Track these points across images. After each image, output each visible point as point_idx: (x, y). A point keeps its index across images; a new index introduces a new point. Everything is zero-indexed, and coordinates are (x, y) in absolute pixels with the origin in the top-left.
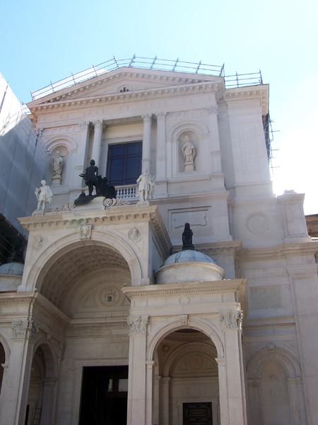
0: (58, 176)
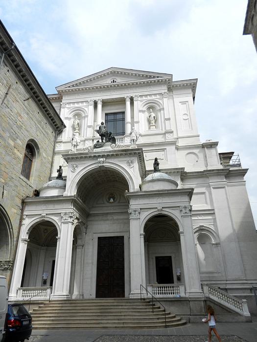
0: (78, 131)
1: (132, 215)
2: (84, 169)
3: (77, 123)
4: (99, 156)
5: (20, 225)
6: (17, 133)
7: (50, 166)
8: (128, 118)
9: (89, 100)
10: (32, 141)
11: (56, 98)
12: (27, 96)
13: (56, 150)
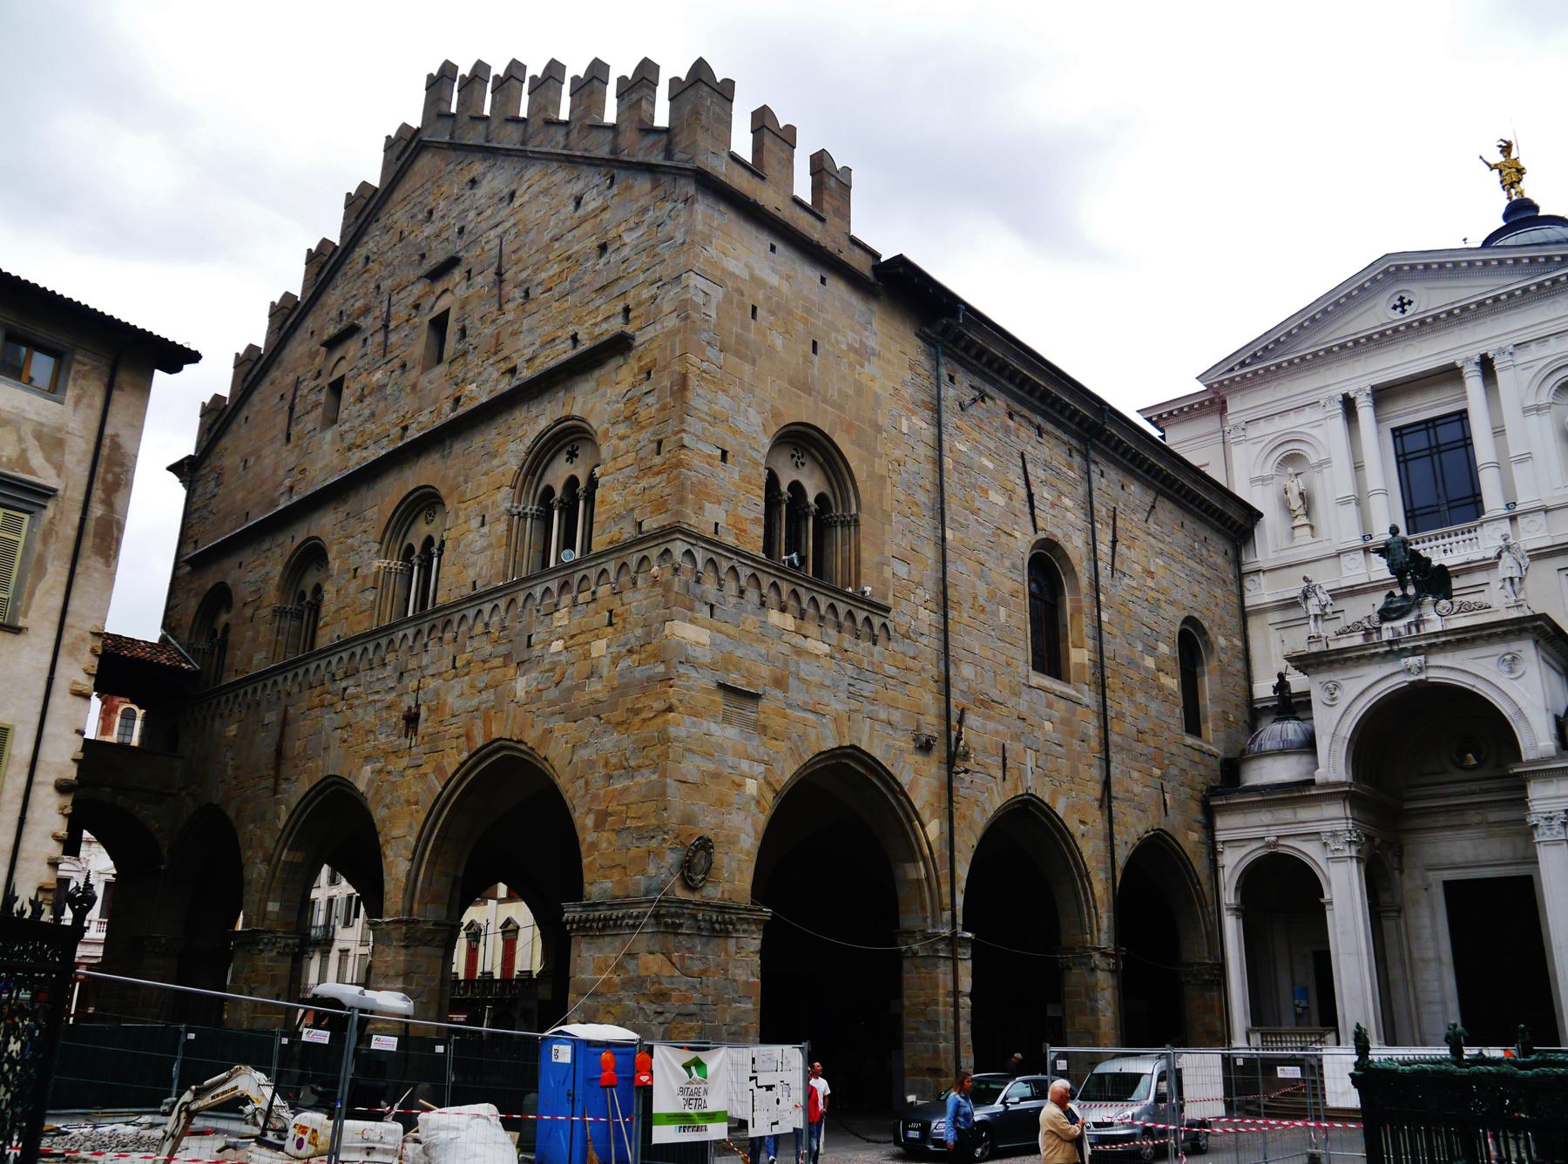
0: (1304, 520)
1: (1540, 831)
2: (1362, 693)
3: (1296, 492)
5: (1215, 868)
6: (1155, 627)
7: (1239, 665)
8: (1483, 448)
9: (1322, 396)
11: (1201, 404)
12: (1149, 498)
13: (1247, 603)
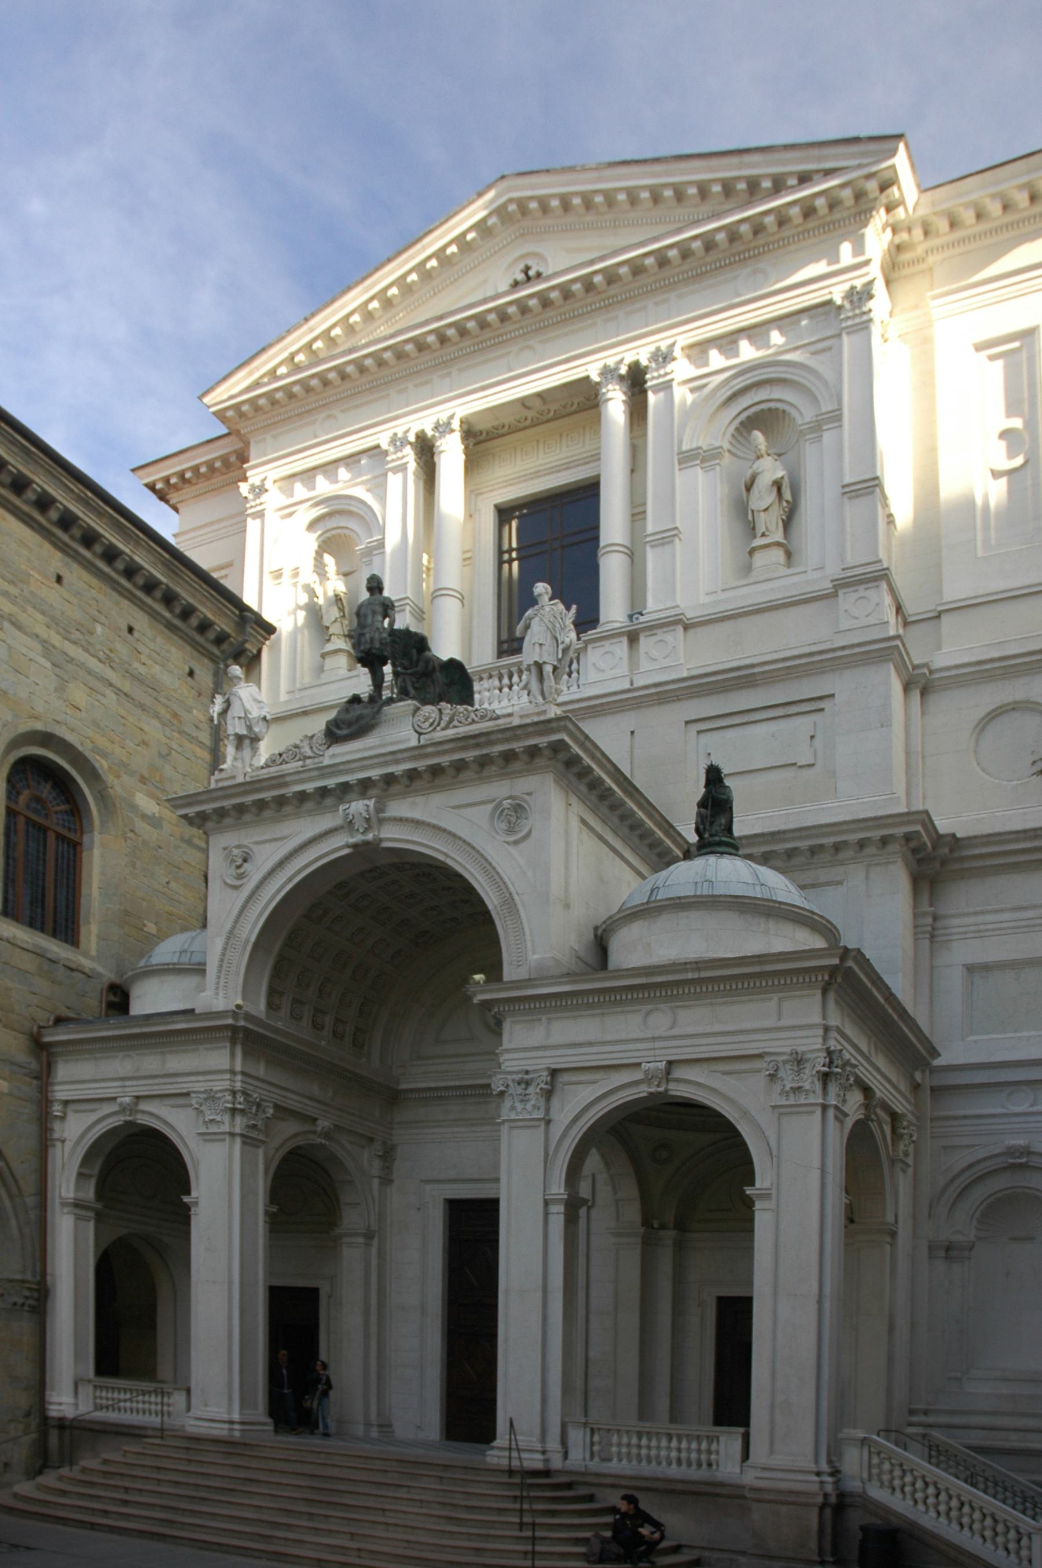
4: (345, 787)
10: (47, 739)
